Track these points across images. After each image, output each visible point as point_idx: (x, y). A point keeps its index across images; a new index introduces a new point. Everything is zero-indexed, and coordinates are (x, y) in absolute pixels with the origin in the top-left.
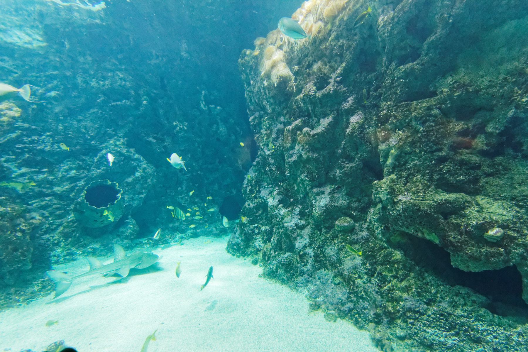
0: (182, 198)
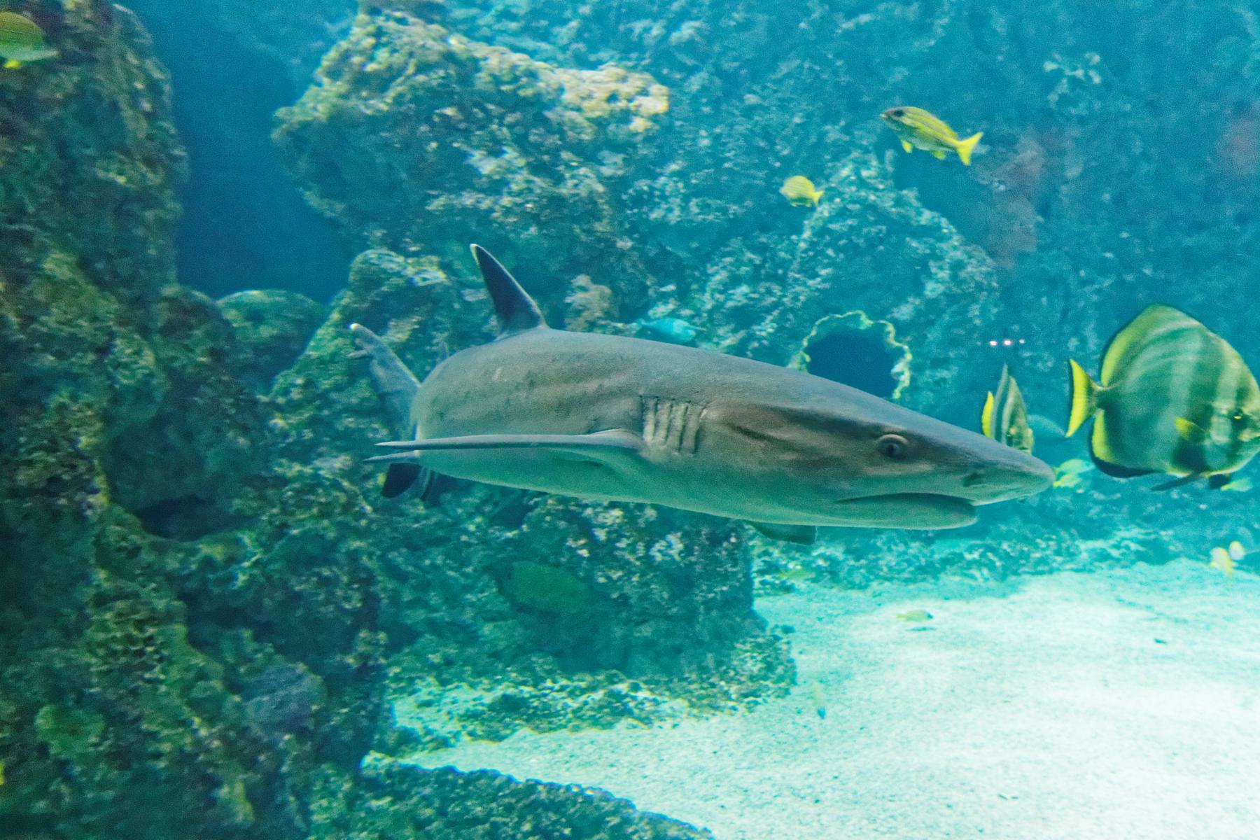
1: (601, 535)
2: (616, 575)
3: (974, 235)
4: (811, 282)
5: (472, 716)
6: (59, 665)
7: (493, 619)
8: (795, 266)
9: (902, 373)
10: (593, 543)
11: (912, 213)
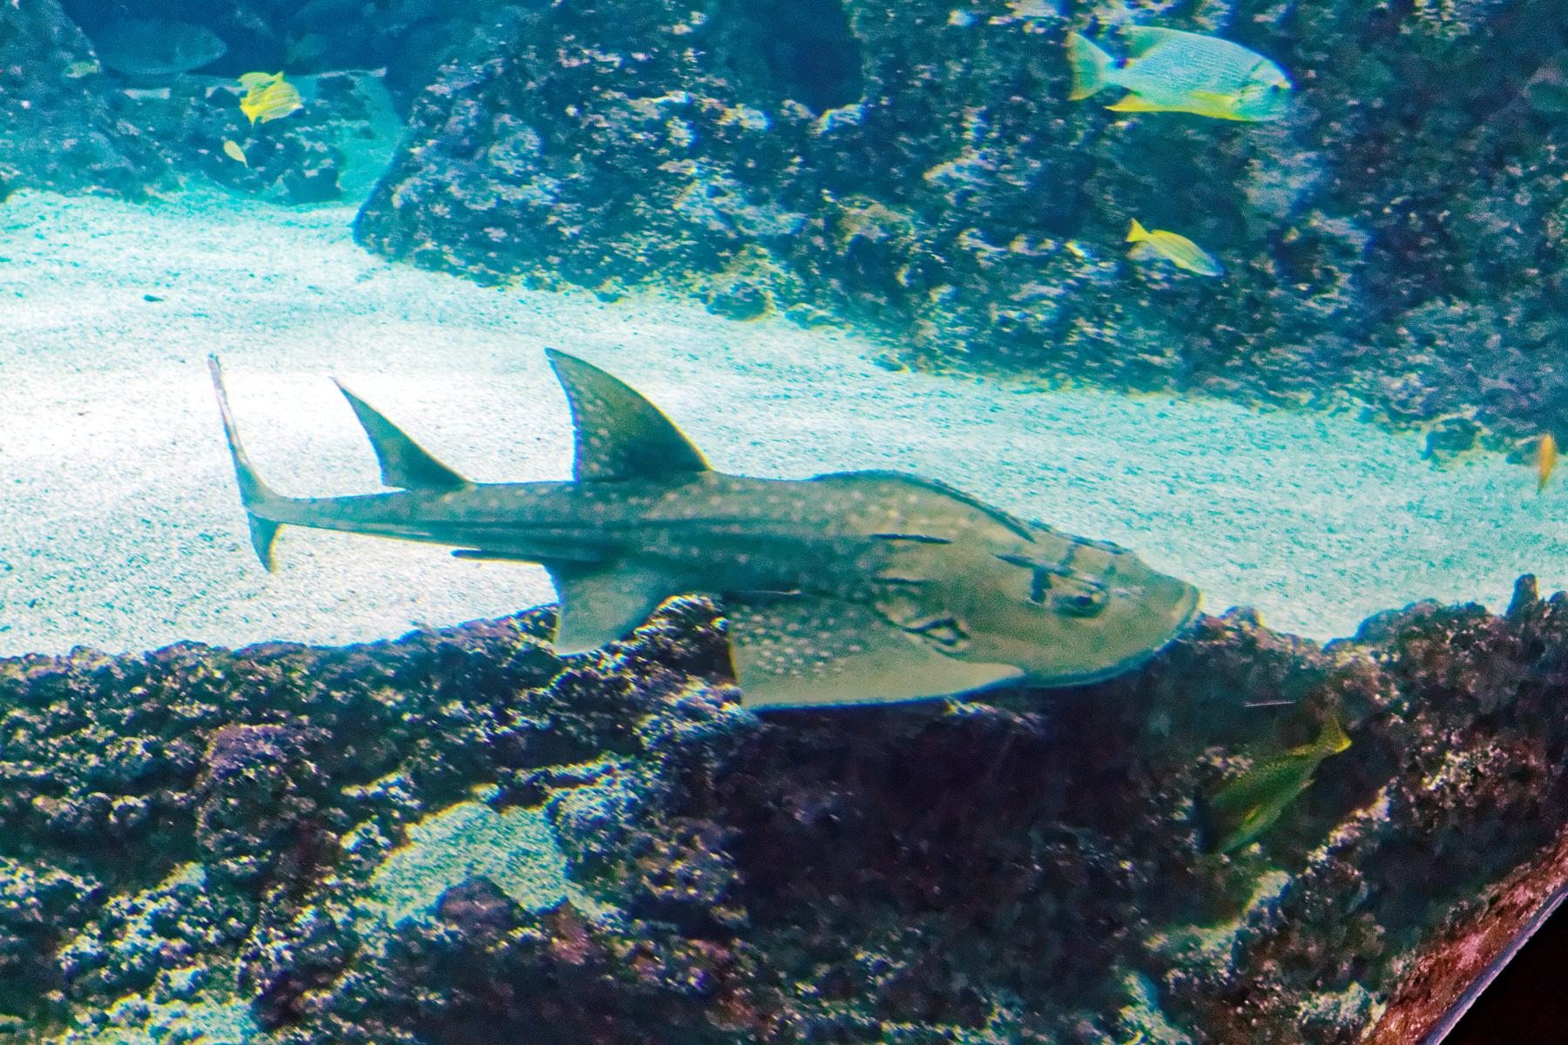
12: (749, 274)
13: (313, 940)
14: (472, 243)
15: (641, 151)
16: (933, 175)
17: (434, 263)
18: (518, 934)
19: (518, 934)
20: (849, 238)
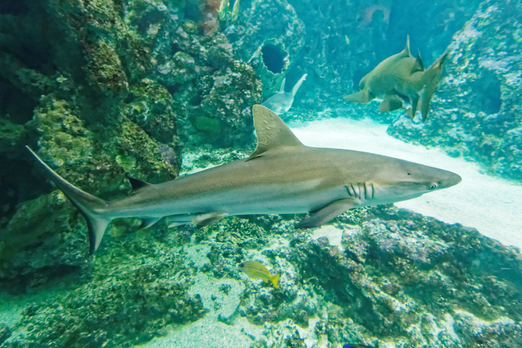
0: (321, 68)
1: (228, 107)
2: (233, 120)
3: (301, 15)
4: (254, 27)
5: (196, 161)
6: (119, 142)
7: (192, 134)
8: (249, 20)
9: (287, 61)
10: (226, 110)
11: (285, 5)
12: (459, 148)
13: (301, 237)
14: (405, 135)
15: (444, 120)
16: (509, 132)
17: (397, 137)
18: (326, 247)
19: (326, 247)
20: (484, 143)
